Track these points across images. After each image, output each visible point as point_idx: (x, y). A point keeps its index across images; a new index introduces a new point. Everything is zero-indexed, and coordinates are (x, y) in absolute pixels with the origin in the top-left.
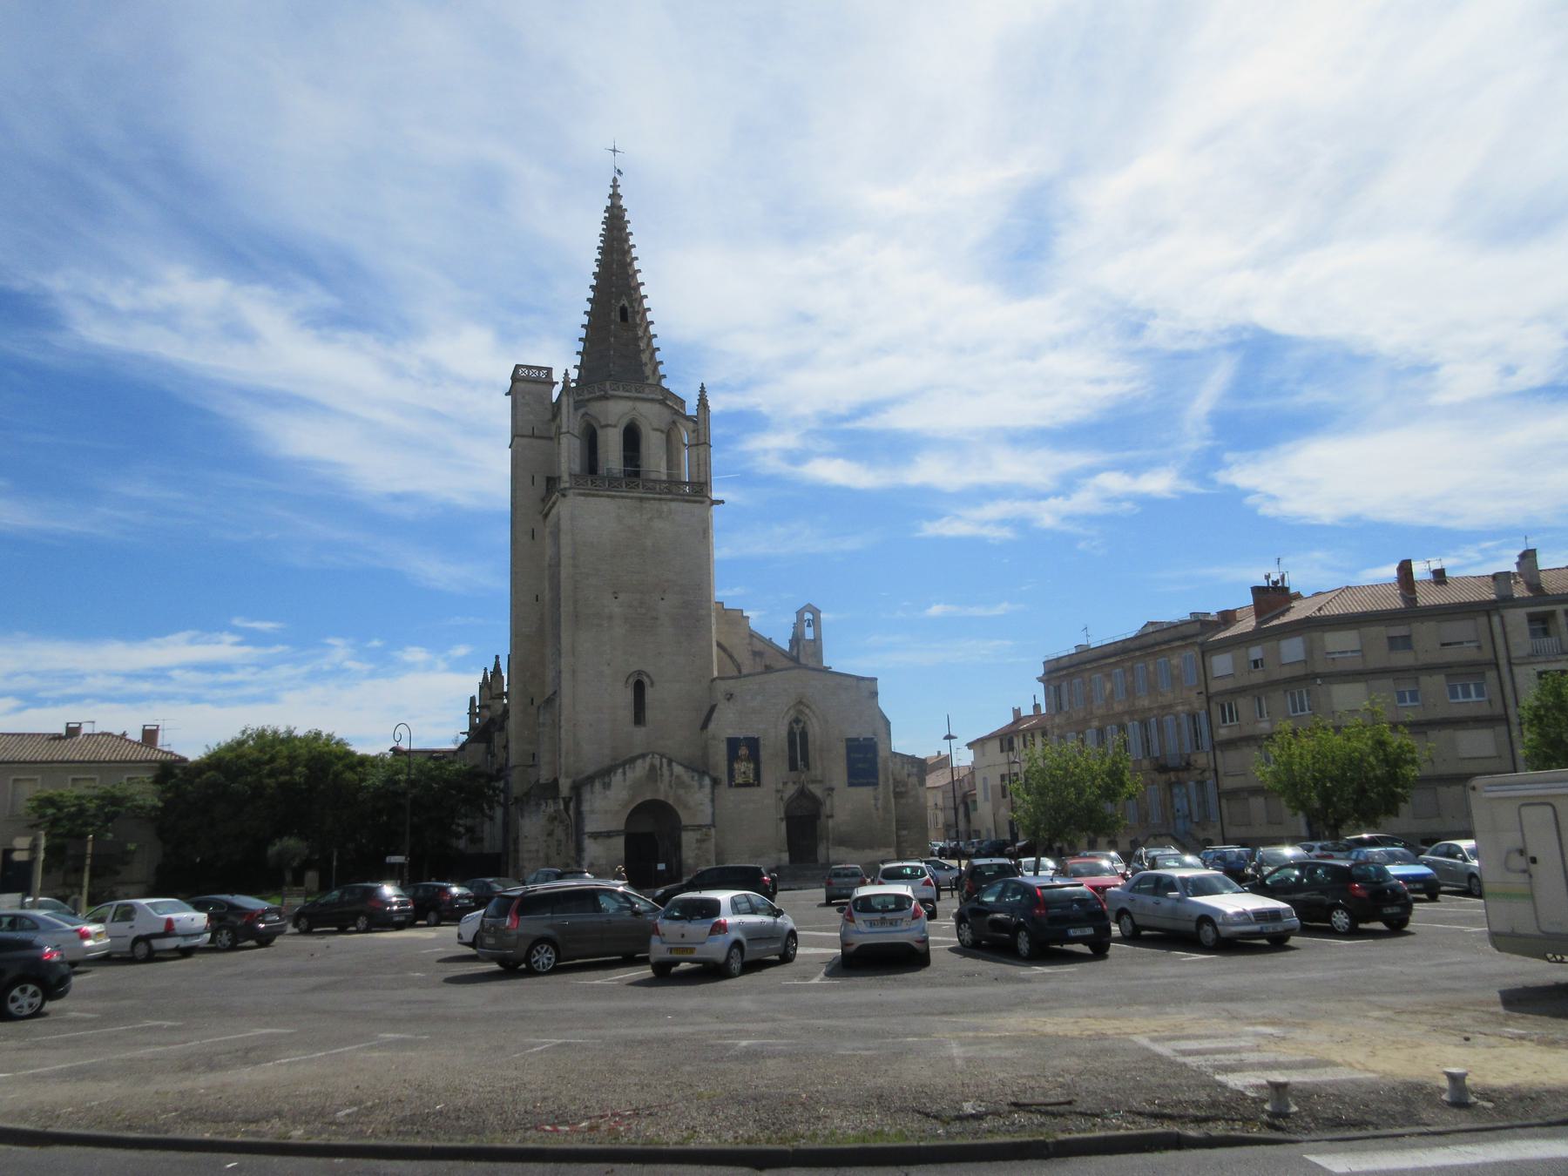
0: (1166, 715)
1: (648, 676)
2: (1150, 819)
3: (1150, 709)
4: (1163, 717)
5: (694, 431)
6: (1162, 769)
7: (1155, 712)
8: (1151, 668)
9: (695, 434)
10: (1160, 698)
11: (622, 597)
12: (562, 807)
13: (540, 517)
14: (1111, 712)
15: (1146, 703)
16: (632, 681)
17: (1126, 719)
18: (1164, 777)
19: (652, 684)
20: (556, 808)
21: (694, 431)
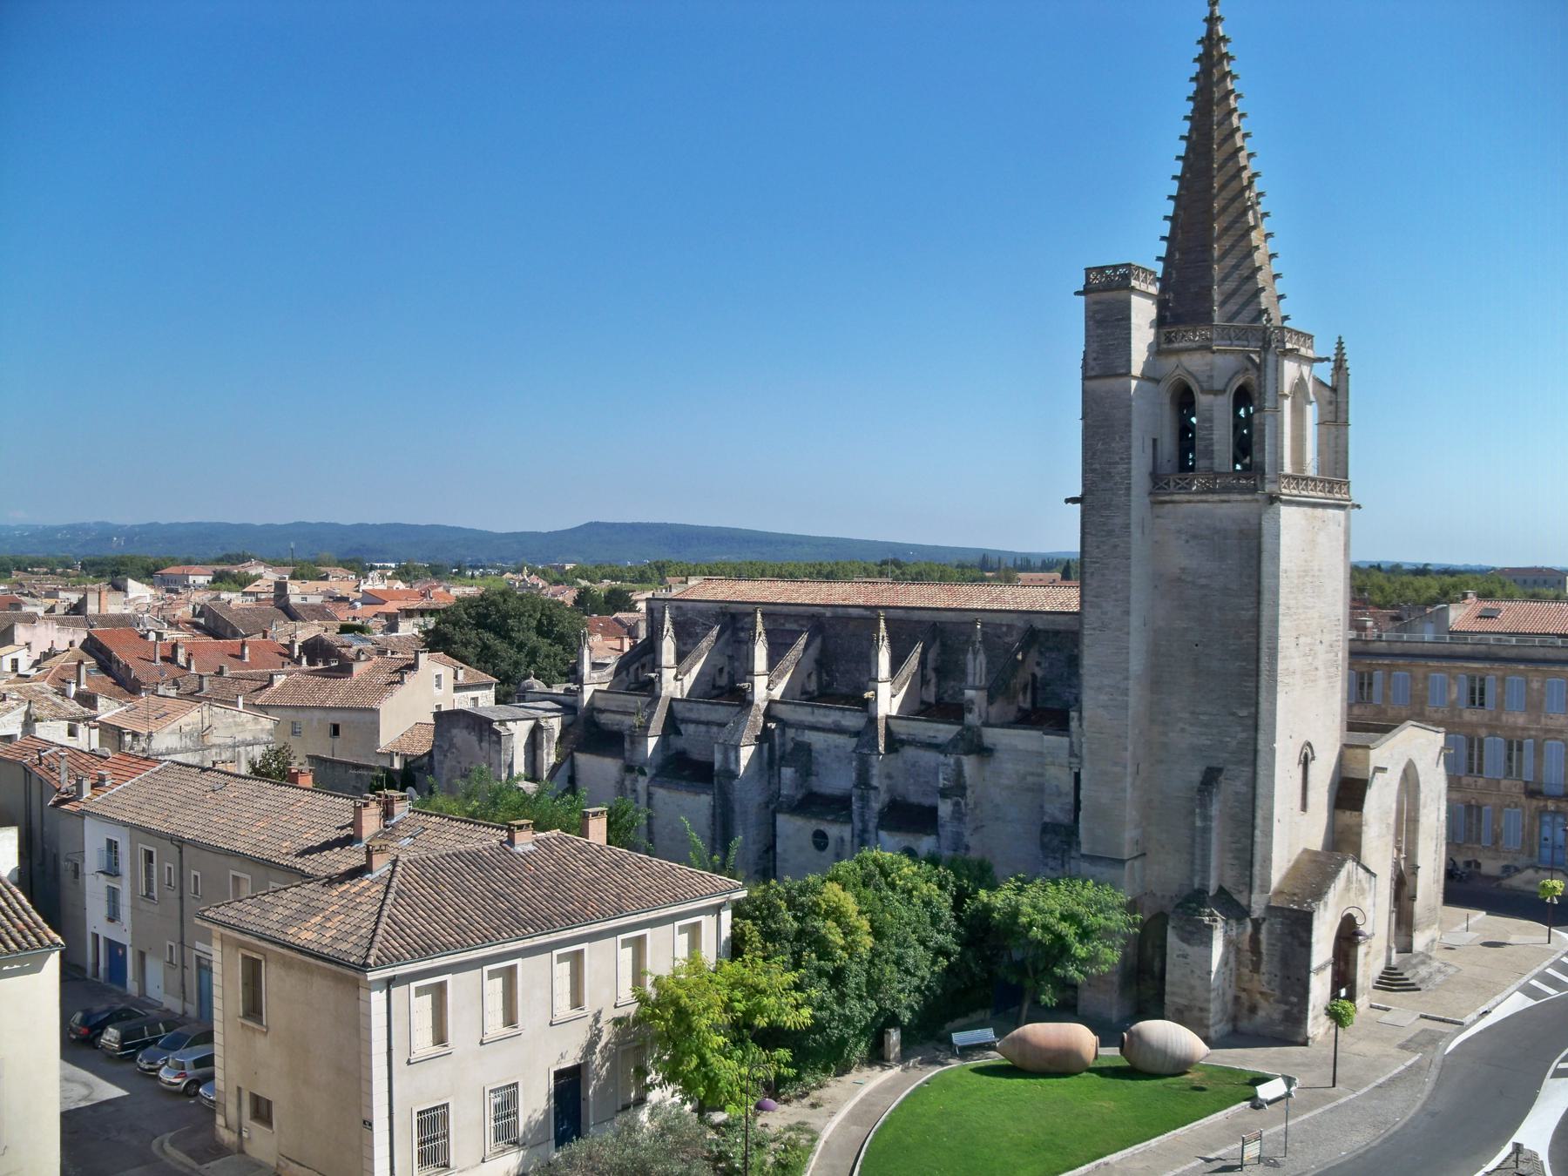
0: (1550, 739)
2: (1501, 843)
3: (1524, 729)
4: (1544, 740)
5: (1330, 403)
6: (1532, 793)
7: (1533, 733)
8: (1535, 685)
9: (1332, 408)
10: (1543, 720)
11: (1302, 640)
12: (1249, 929)
13: (1147, 500)
14: (1456, 720)
15: (1521, 720)
17: (1483, 732)
18: (1535, 803)
19: (1313, 758)
21: (1330, 403)
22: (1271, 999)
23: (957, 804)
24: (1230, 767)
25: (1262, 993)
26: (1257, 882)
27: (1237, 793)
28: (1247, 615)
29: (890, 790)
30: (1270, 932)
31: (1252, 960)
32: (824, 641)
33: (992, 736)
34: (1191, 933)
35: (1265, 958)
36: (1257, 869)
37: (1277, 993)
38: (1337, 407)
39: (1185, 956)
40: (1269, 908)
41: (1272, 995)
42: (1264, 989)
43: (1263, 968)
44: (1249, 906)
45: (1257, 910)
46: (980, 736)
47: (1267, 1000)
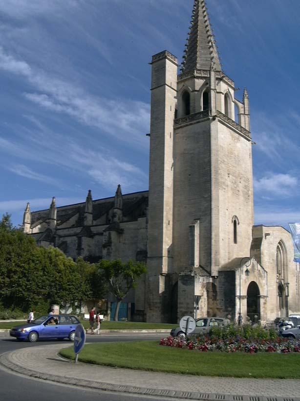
1: (238, 220)
9: (243, 109)
11: (230, 176)
16: (233, 220)
19: (239, 224)
20: (207, 281)
22: (221, 311)
23: (108, 249)
24: (202, 217)
25: (217, 309)
26: (213, 261)
27: (205, 227)
28: (206, 160)
29: (89, 251)
30: (220, 282)
31: (213, 295)
32: (80, 215)
33: (122, 225)
34: (187, 281)
35: (218, 293)
36: (213, 256)
37: (223, 307)
38: (244, 109)
39: (185, 291)
40: (219, 272)
41: (221, 309)
42: (219, 307)
43: (218, 298)
44: (211, 271)
45: (215, 273)
46: (119, 226)
47: (219, 311)
